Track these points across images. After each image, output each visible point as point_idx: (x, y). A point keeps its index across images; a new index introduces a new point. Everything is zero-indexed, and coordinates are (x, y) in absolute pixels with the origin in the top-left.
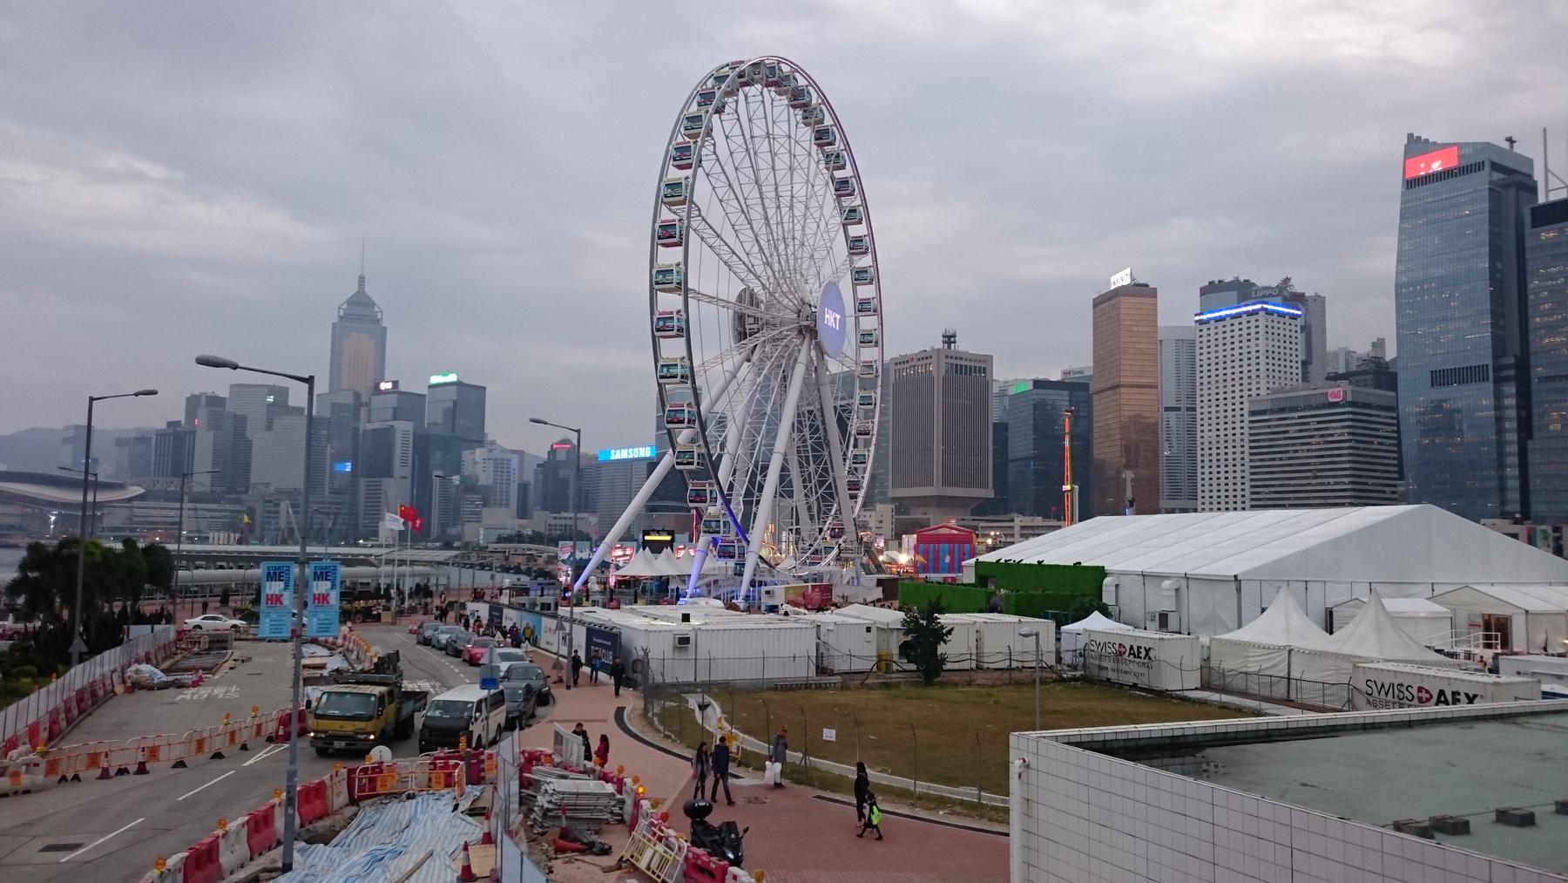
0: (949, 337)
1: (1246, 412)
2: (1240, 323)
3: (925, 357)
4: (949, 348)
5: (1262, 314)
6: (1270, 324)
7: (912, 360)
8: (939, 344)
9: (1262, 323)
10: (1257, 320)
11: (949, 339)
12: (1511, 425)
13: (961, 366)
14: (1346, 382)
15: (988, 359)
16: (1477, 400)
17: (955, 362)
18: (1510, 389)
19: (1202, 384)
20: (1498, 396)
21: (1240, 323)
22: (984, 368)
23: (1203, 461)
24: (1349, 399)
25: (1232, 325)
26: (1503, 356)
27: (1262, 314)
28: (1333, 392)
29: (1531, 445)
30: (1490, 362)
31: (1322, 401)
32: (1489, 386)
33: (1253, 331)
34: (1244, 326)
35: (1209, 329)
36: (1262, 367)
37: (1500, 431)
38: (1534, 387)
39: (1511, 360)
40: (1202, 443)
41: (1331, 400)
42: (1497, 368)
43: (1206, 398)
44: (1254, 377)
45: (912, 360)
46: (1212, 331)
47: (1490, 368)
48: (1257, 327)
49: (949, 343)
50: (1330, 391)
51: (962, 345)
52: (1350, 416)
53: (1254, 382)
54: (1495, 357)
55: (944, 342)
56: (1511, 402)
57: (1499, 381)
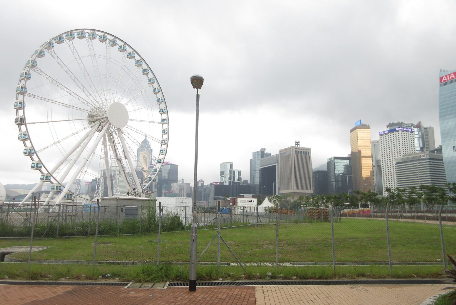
0: (297, 143)
2: (393, 135)
3: (289, 149)
4: (298, 146)
5: (400, 131)
7: (285, 150)
8: (294, 145)
9: (400, 134)
10: (398, 133)
11: (297, 143)
15: (309, 149)
17: (298, 150)
22: (308, 152)
25: (391, 135)
44: (399, 152)
45: (285, 150)
46: (385, 138)
48: (399, 135)
51: (302, 145)
53: (399, 154)
55: (296, 144)
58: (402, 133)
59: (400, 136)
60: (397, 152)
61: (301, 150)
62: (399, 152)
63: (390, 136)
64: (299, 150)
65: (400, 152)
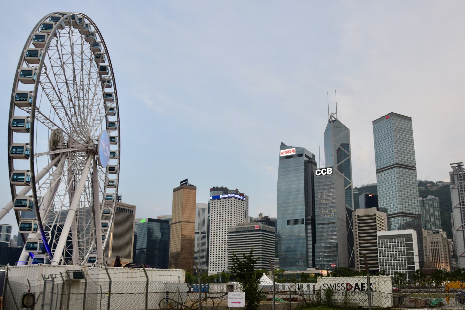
1: (227, 232)
2: (226, 201)
4: (118, 201)
5: (233, 198)
6: (235, 202)
9: (233, 201)
10: (231, 200)
12: (310, 239)
13: (123, 209)
14: (260, 223)
15: (134, 207)
16: (300, 230)
17: (120, 207)
18: (310, 227)
19: (212, 222)
20: (307, 229)
21: (226, 201)
22: (132, 211)
23: (211, 250)
24: (261, 229)
26: (308, 216)
27: (233, 198)
28: (256, 226)
29: (316, 245)
30: (304, 218)
31: (253, 229)
32: (304, 225)
33: (230, 204)
34: (227, 202)
35: (215, 202)
36: (233, 217)
37: (307, 240)
38: (316, 227)
39: (310, 217)
40: (211, 243)
41: (256, 229)
42: (307, 220)
43: (213, 227)
44: (230, 220)
46: (216, 203)
47: (304, 220)
48: (231, 202)
49: (119, 199)
50: (255, 226)
52: (262, 235)
53: (230, 222)
54: (306, 216)
56: (310, 231)
57: (307, 224)
58: (235, 200)
59: (233, 203)
60: (228, 220)
61: (124, 208)
62: (230, 220)
63: (227, 202)
64: (122, 207)
65: (231, 220)
